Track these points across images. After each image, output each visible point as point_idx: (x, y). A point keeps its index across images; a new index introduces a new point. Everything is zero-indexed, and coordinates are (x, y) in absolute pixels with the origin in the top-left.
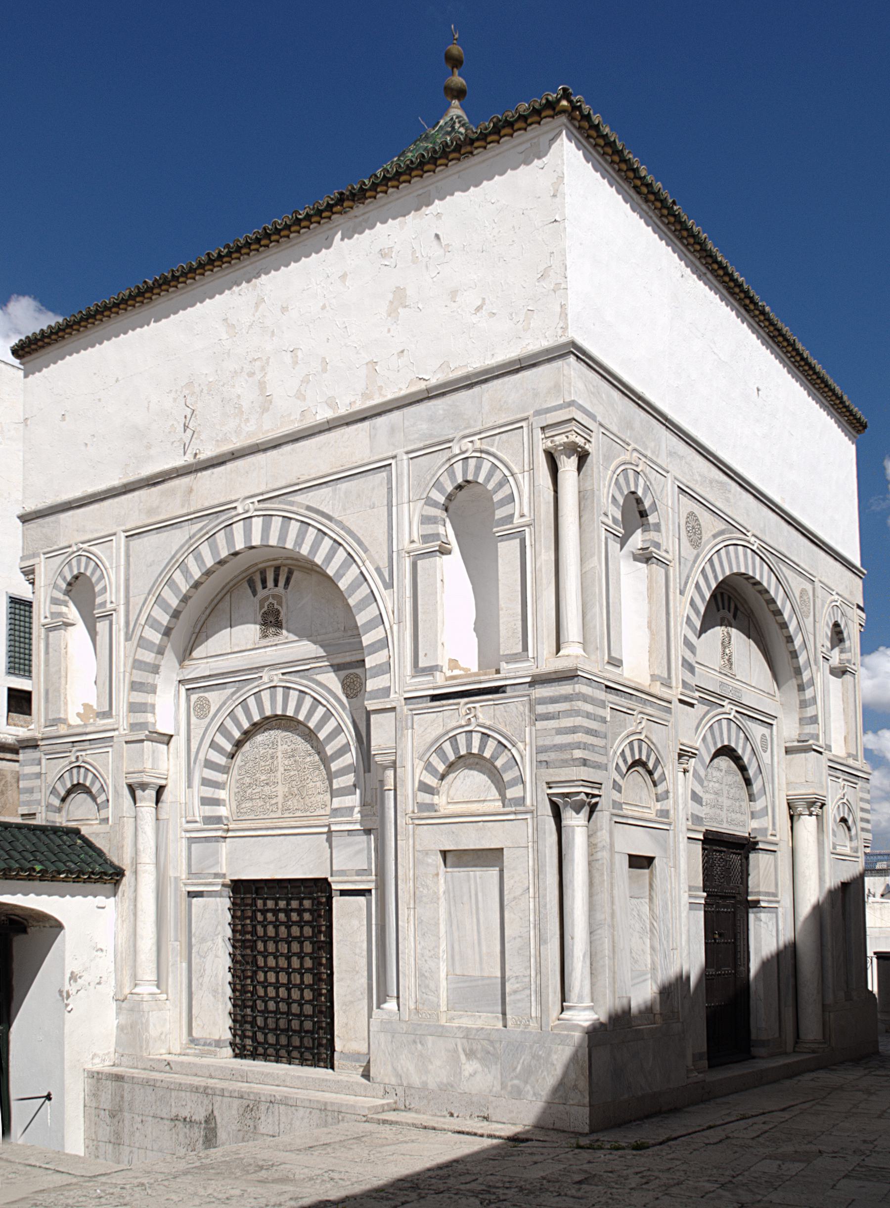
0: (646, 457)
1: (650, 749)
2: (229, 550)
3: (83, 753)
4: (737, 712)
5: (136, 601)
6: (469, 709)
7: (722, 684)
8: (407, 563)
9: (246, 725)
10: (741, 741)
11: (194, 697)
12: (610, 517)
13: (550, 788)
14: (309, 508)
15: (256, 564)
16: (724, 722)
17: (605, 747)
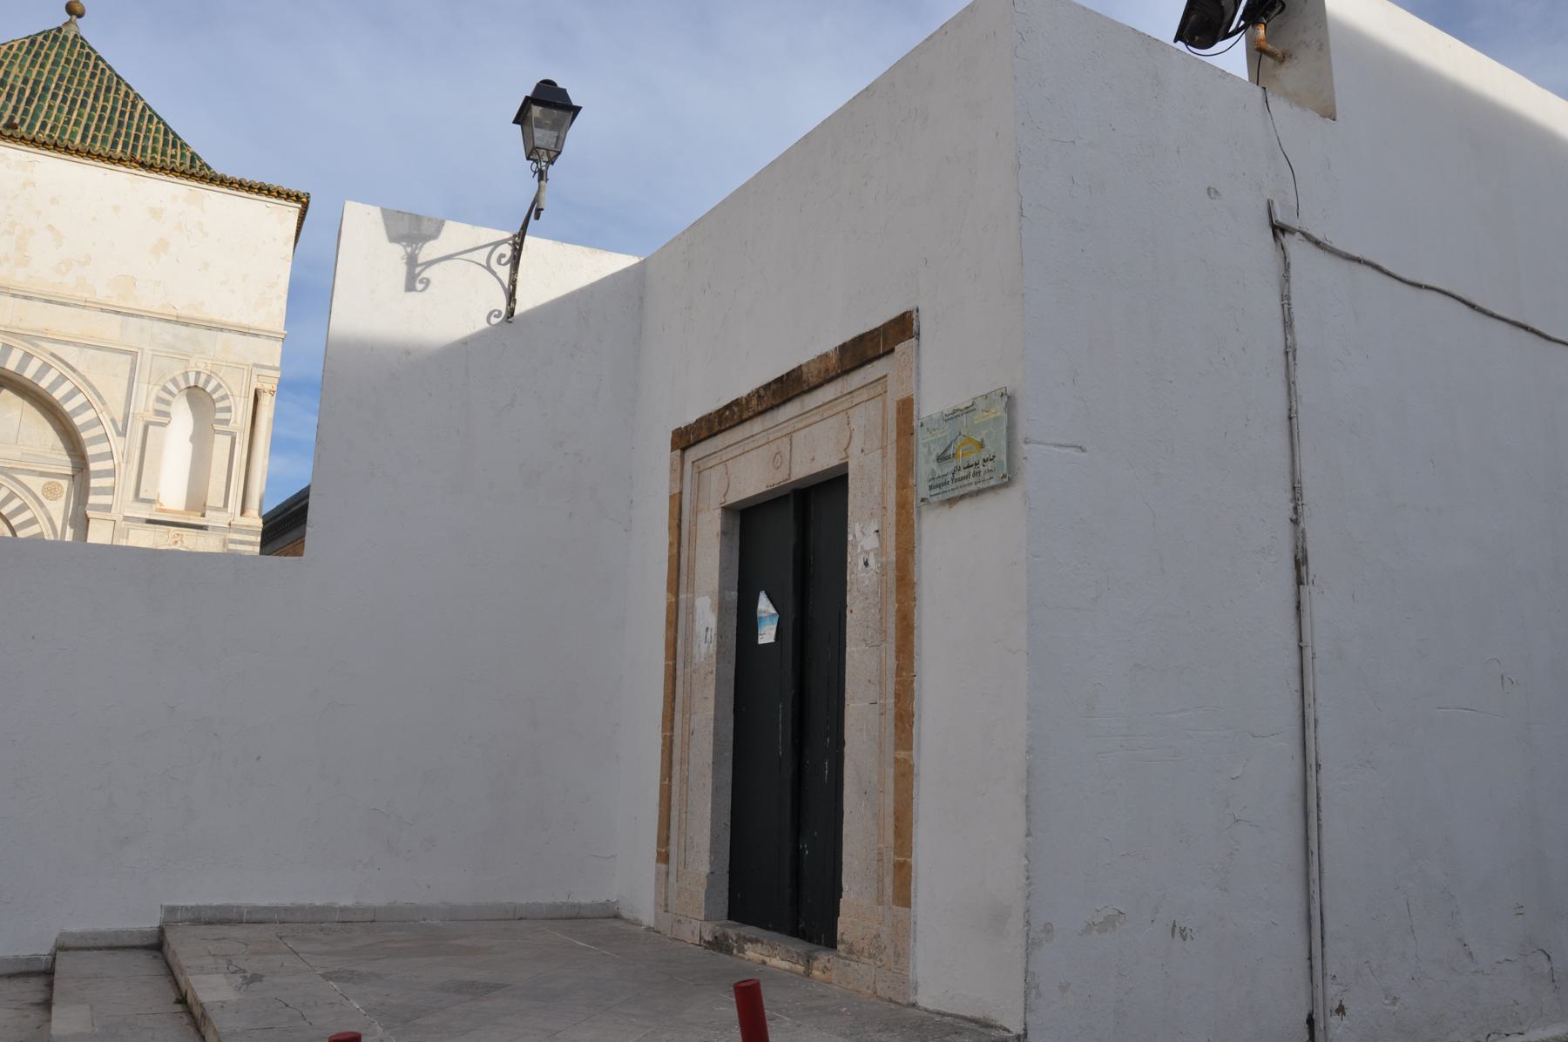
6: (178, 535)
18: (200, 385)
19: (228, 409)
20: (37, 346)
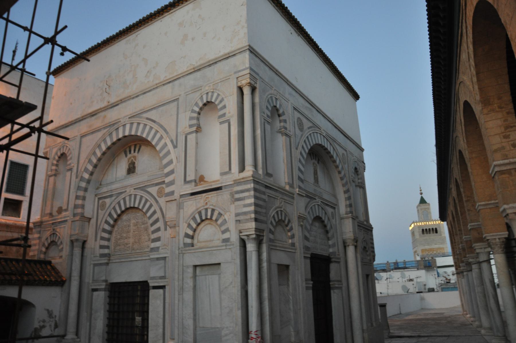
0: (280, 93)
1: (286, 215)
4: (321, 202)
7: (315, 190)
10: (324, 214)
11: (101, 201)
12: (266, 114)
13: (241, 233)
16: (317, 206)
17: (265, 213)
18: (209, 100)
19: (224, 107)
20: (141, 117)
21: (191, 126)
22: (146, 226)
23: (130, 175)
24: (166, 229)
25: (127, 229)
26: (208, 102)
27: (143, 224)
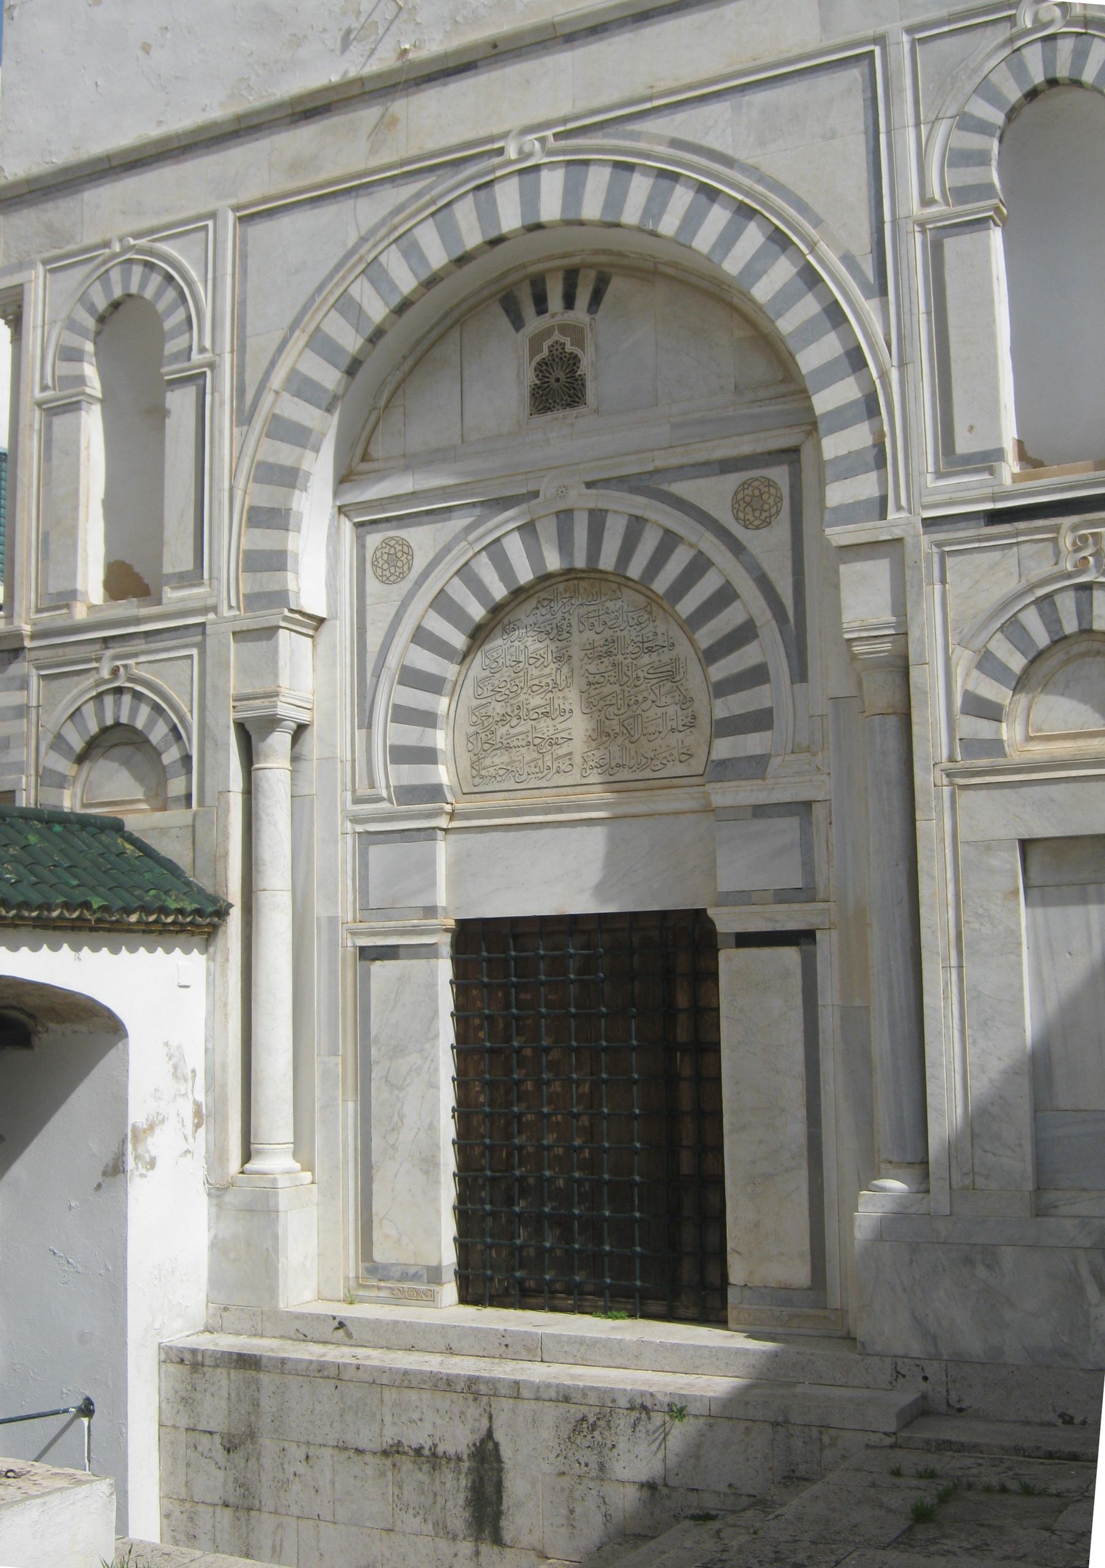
2: (483, 232)
3: (131, 662)
5: (261, 345)
6: (1084, 538)
8: (917, 246)
9: (499, 591)
11: (374, 540)
14: (675, 143)
15: (524, 266)
18: (1062, 71)
20: (636, 136)
21: (961, 194)
22: (666, 656)
23: (549, 416)
24: (800, 673)
25: (547, 671)
26: (1052, 82)
27: (650, 650)
